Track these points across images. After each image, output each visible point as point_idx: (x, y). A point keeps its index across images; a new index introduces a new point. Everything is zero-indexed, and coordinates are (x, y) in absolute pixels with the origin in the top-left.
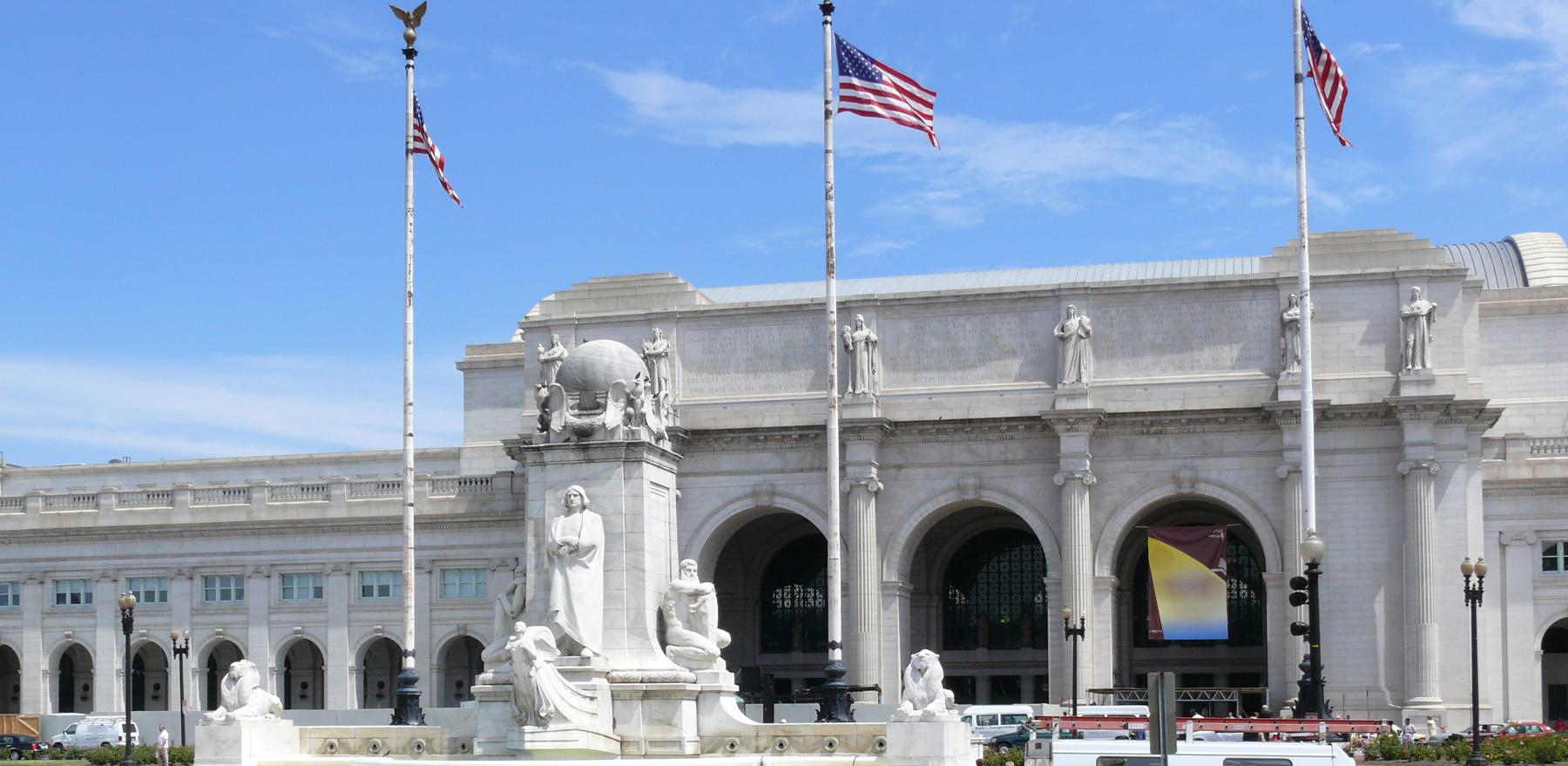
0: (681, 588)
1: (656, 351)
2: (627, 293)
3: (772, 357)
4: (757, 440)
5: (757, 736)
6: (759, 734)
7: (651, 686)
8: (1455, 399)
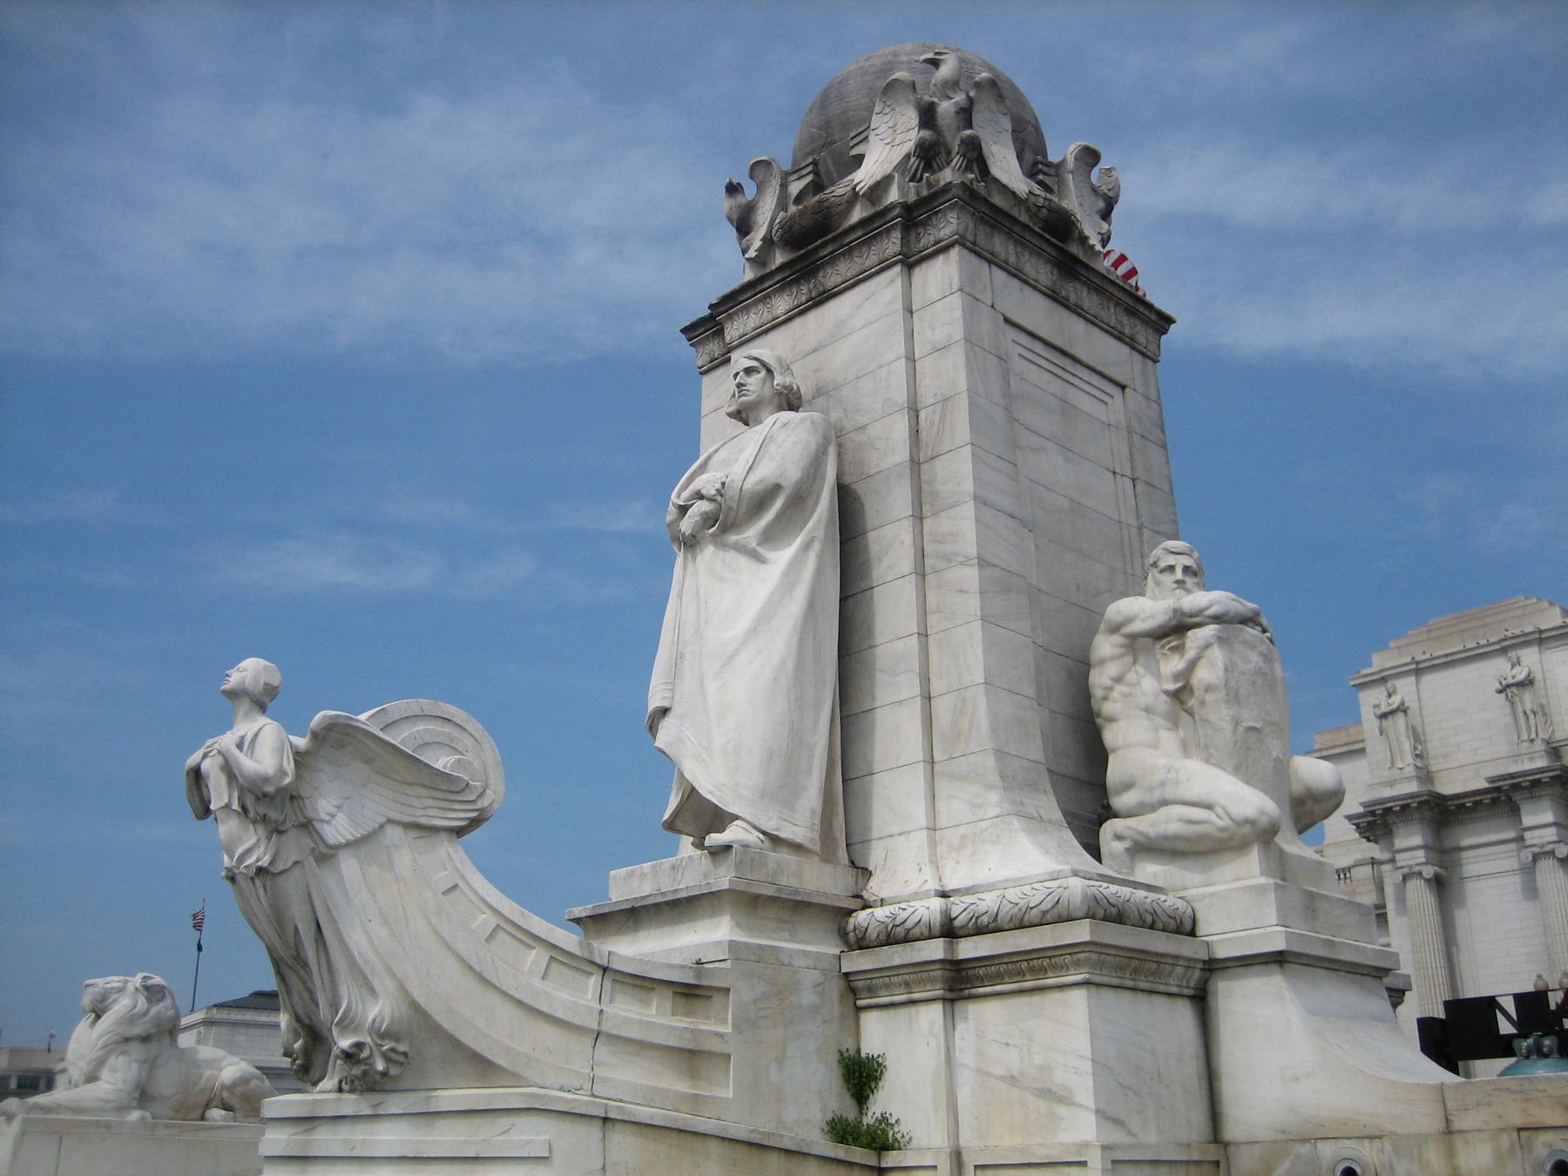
0: (1130, 620)
5: (1449, 1132)
6: (1457, 1125)
7: (969, 949)
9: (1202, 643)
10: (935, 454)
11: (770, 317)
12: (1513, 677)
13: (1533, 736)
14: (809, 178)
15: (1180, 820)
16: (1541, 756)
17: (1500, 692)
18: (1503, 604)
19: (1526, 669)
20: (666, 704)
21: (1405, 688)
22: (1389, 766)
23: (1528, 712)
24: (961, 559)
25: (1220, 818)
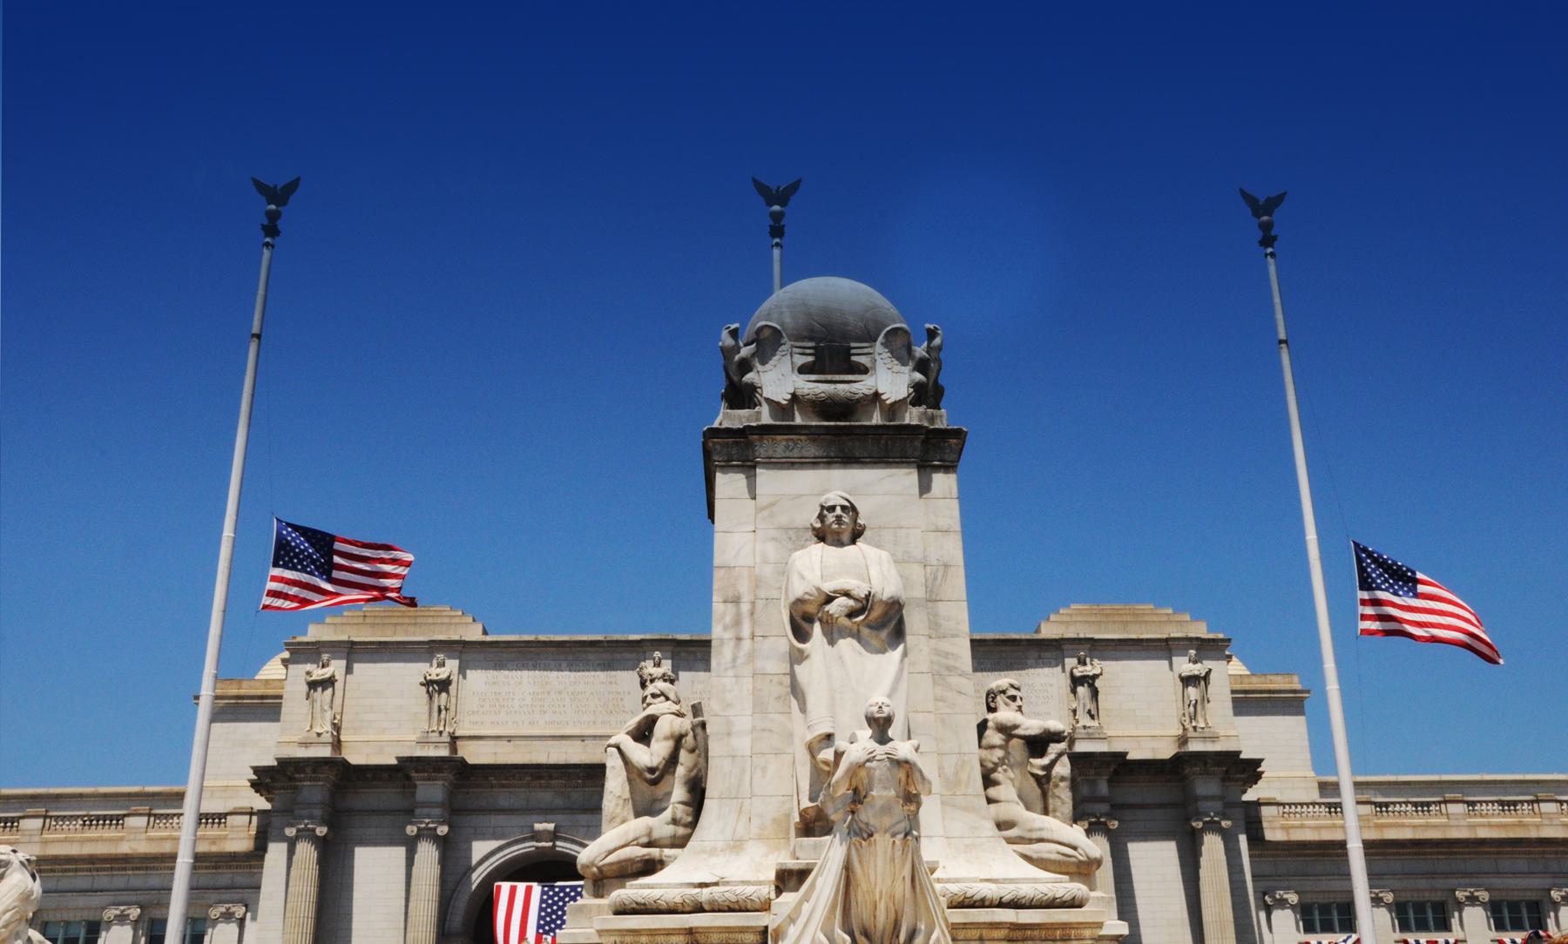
0: (1016, 727)
1: (439, 677)
2: (407, 621)
3: (560, 693)
4: (540, 778)
8: (1242, 756)
9: (1059, 751)
10: (938, 598)
11: (800, 456)
12: (437, 675)
13: (441, 728)
14: (811, 359)
15: (1059, 853)
16: (446, 747)
17: (422, 684)
18: (431, 609)
19: (449, 670)
20: (829, 730)
21: (336, 667)
22: (308, 728)
23: (442, 707)
24: (959, 672)
25: (1081, 855)
